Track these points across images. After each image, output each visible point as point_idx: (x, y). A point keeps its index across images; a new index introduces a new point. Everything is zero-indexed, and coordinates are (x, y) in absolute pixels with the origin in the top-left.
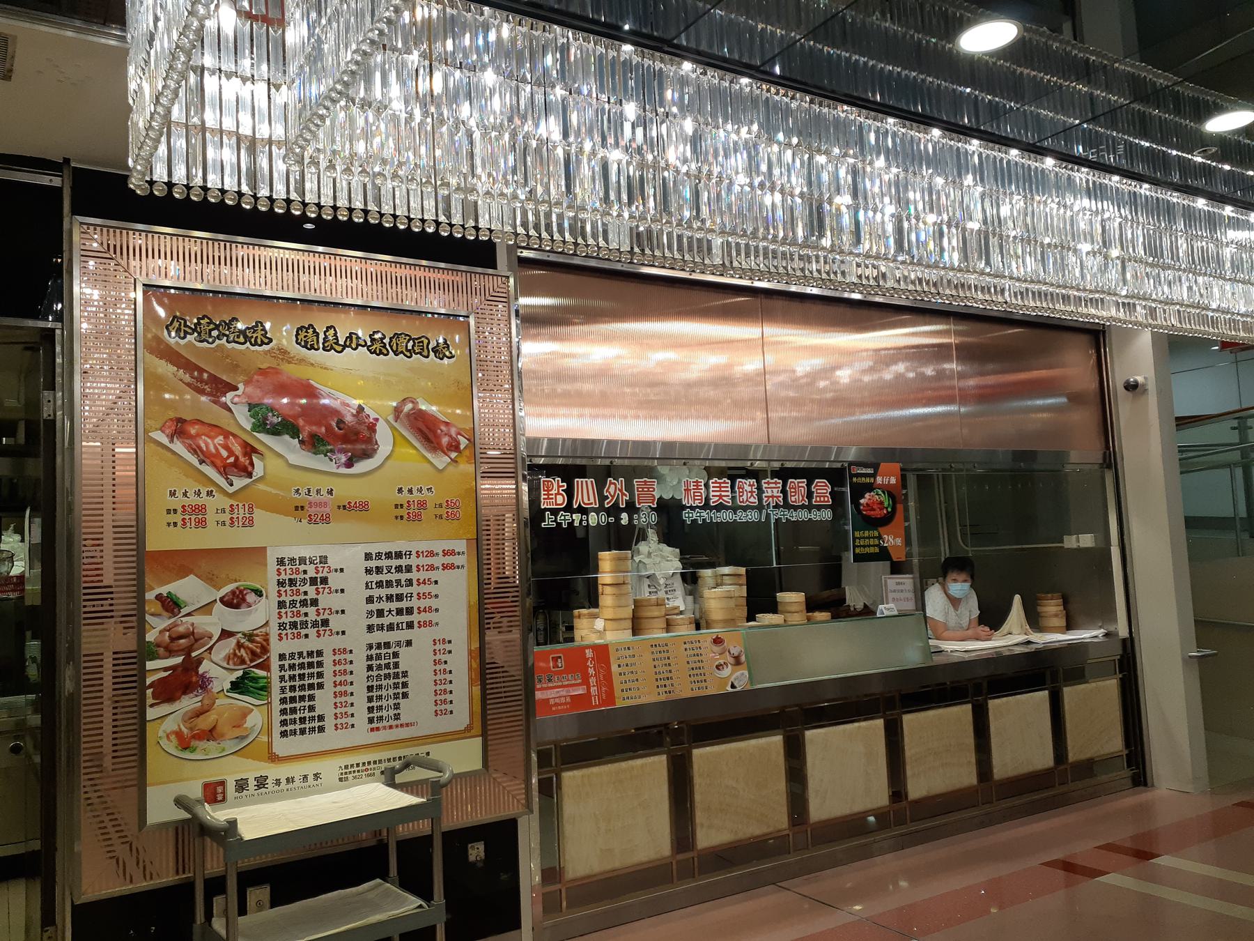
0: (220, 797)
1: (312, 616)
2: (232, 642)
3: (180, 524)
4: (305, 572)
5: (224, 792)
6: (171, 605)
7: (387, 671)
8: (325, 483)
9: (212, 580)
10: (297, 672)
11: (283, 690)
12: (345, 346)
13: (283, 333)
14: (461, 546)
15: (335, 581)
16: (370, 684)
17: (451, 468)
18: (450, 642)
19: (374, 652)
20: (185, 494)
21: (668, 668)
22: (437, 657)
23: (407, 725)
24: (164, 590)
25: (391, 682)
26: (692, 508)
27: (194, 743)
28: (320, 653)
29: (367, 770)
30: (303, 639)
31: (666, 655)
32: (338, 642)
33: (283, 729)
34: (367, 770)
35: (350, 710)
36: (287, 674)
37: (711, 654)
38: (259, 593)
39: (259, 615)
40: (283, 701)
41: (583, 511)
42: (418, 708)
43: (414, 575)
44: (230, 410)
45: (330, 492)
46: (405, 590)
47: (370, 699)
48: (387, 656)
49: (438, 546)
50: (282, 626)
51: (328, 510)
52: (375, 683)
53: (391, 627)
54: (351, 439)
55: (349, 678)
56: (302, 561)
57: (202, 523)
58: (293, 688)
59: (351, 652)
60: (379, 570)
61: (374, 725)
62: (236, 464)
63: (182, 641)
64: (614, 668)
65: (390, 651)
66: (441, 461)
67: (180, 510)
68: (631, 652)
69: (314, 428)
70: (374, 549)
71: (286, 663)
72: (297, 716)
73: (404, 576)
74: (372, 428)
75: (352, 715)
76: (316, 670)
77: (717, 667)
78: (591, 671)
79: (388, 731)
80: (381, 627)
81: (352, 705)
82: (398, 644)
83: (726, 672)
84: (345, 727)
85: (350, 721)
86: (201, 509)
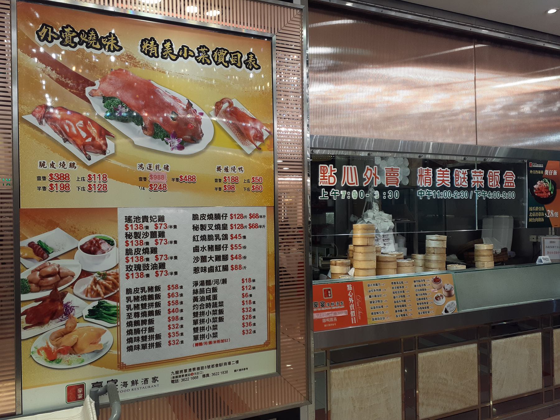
1: (152, 261)
2: (90, 279)
3: (48, 188)
6: (41, 251)
7: (208, 302)
8: (162, 161)
9: (73, 232)
10: (140, 303)
11: (129, 316)
12: (178, 56)
13: (131, 45)
14: (262, 211)
15: (170, 234)
16: (195, 311)
17: (257, 154)
18: (254, 281)
19: (198, 287)
20: (52, 165)
21: (403, 299)
22: (245, 292)
23: (222, 341)
24: (35, 239)
25: (211, 309)
26: (424, 188)
27: (59, 356)
28: (158, 288)
29: (192, 374)
30: (145, 278)
31: (402, 289)
32: (172, 280)
34: (192, 374)
35: (180, 330)
36: (132, 304)
37: (432, 290)
38: (111, 243)
39: (111, 259)
40: (129, 324)
41: (348, 188)
42: (230, 328)
43: (229, 232)
44: (88, 101)
45: (167, 168)
46: (222, 243)
47: (195, 322)
49: (246, 211)
50: (129, 268)
51: (164, 181)
52: (199, 311)
53: (211, 269)
54: (185, 133)
55: (180, 307)
56: (145, 218)
57: (65, 188)
58: (137, 315)
59: (181, 287)
60: (203, 227)
61: (198, 341)
63: (50, 279)
64: (367, 298)
65: (211, 287)
66: (249, 148)
67: (48, 178)
68: (378, 287)
70: (199, 212)
71: (132, 296)
72: (140, 335)
73: (221, 232)
75: (182, 334)
76: (154, 301)
77: (436, 298)
78: (351, 300)
80: (204, 270)
81: (182, 326)
82: (217, 282)
83: (442, 301)
84: (176, 343)
85: (180, 338)
86: (65, 177)
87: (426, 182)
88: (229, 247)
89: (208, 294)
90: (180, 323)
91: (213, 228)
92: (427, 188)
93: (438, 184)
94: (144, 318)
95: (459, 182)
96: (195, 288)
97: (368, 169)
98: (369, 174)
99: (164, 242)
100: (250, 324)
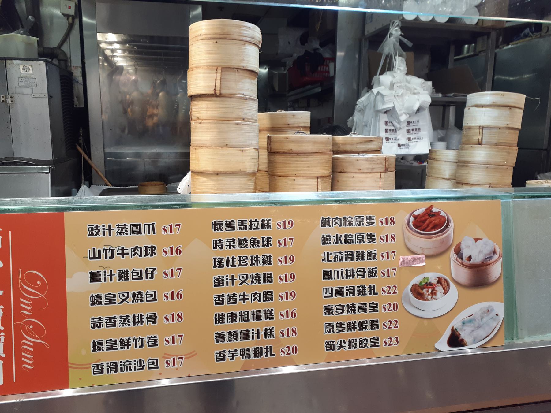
21: (262, 288)
31: (261, 252)
37: (404, 256)
64: (77, 283)
68: (143, 240)
77: (418, 292)
83: (441, 304)
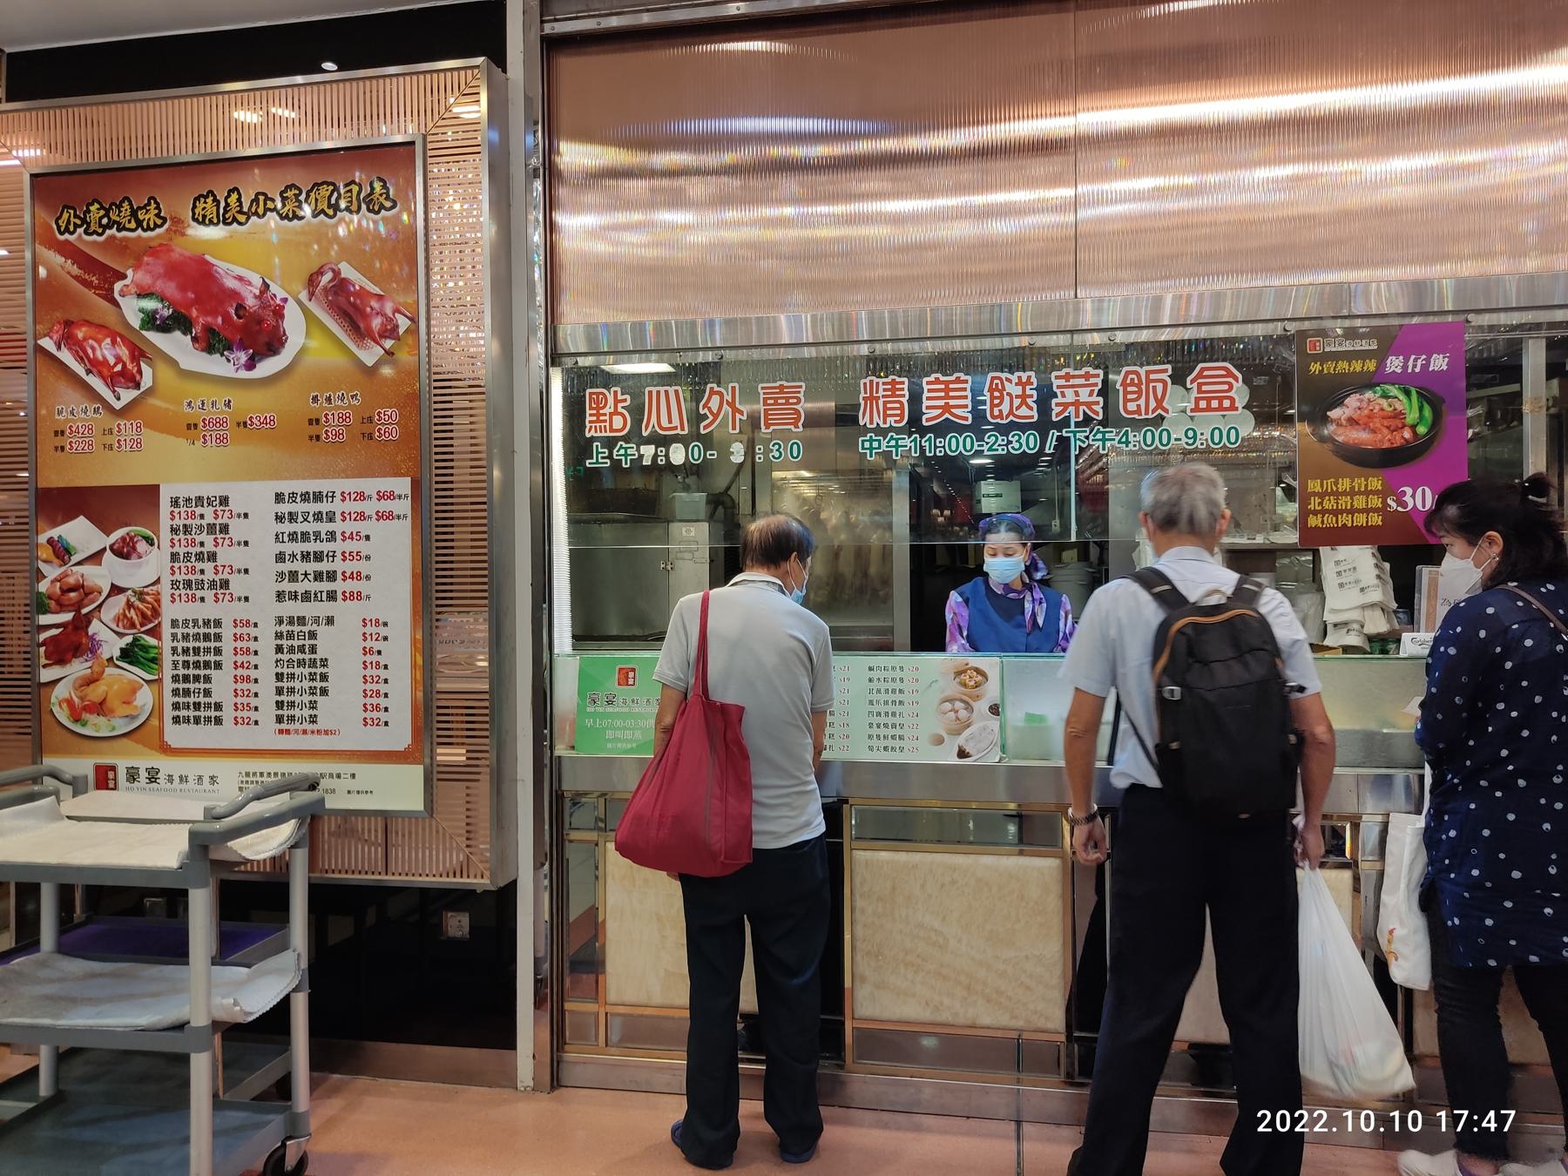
0: (111, 785)
1: (209, 575)
2: (121, 600)
4: (202, 516)
5: (115, 779)
7: (301, 656)
10: (191, 645)
11: (175, 664)
14: (403, 485)
15: (238, 529)
16: (279, 670)
18: (385, 624)
22: (368, 644)
23: (326, 732)
25: (306, 671)
26: (880, 431)
28: (218, 623)
30: (198, 603)
32: (241, 611)
33: (177, 713)
35: (254, 702)
36: (180, 645)
40: (175, 679)
41: (662, 441)
42: (341, 713)
44: (117, 304)
46: (326, 547)
48: (301, 635)
50: (174, 584)
52: (285, 671)
53: (307, 597)
55: (253, 659)
59: (256, 625)
60: (292, 517)
61: (284, 726)
62: (124, 373)
65: (305, 629)
69: (209, 319)
70: (286, 487)
71: (179, 631)
73: (324, 527)
74: (279, 313)
76: (212, 645)
79: (301, 736)
82: (317, 620)
84: (247, 722)
85: (254, 715)
87: (886, 416)
88: (339, 556)
89: (301, 643)
90: (254, 688)
91: (311, 518)
92: (891, 428)
93: (929, 416)
94: (197, 672)
95: (1005, 408)
96: (279, 629)
97: (712, 392)
98: (716, 399)
99: (227, 542)
100: (377, 708)
